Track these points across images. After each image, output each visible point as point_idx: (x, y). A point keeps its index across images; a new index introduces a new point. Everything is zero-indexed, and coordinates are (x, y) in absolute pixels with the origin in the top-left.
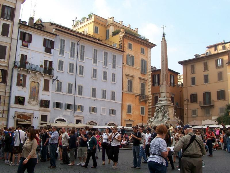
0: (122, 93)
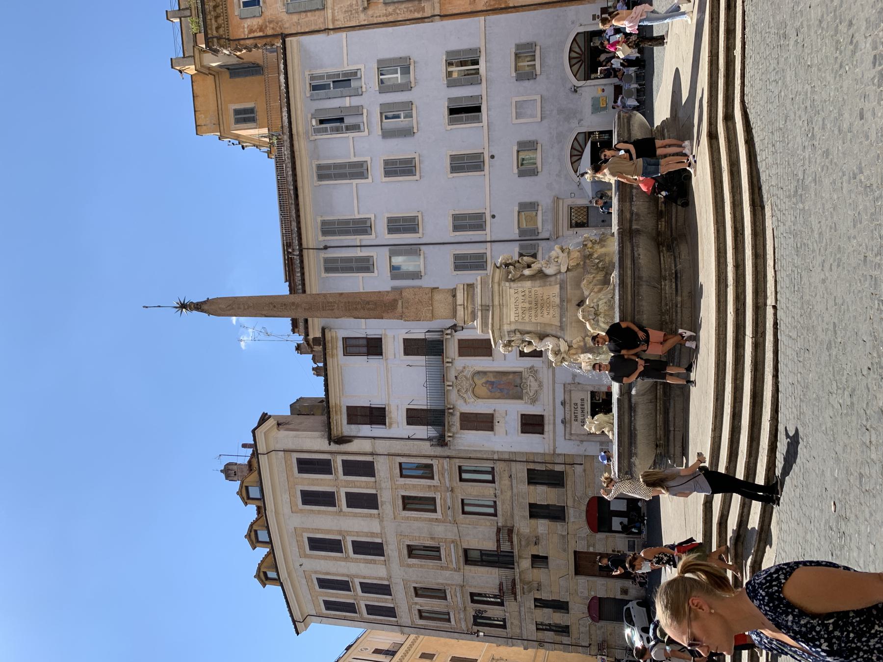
0: (443, 17)
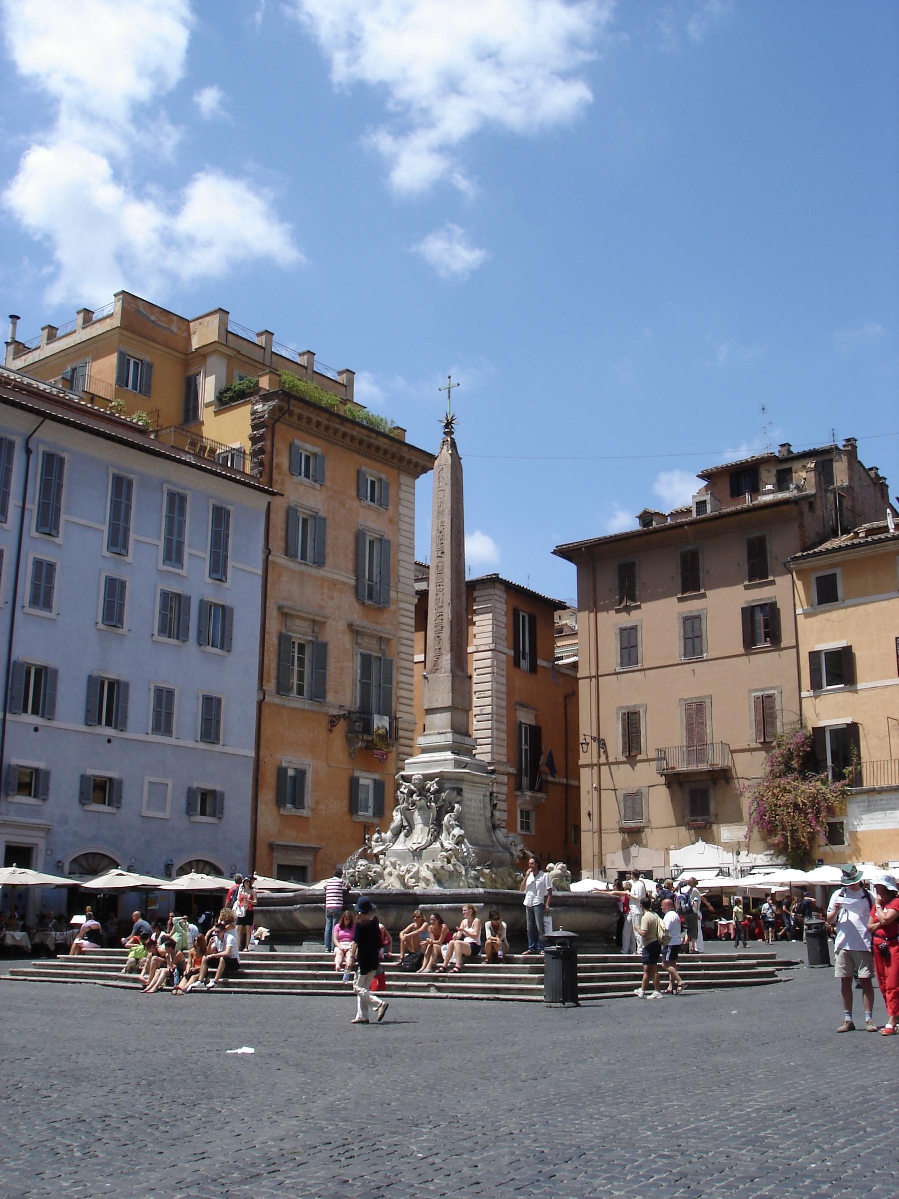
0: (260, 704)
